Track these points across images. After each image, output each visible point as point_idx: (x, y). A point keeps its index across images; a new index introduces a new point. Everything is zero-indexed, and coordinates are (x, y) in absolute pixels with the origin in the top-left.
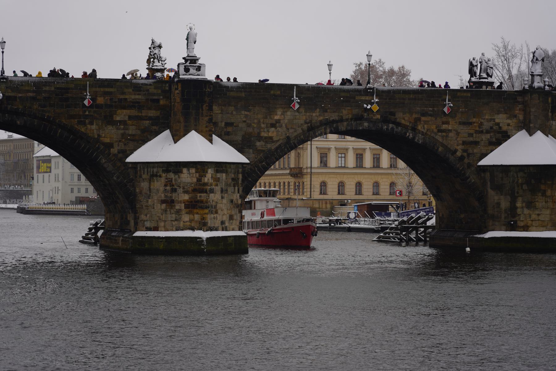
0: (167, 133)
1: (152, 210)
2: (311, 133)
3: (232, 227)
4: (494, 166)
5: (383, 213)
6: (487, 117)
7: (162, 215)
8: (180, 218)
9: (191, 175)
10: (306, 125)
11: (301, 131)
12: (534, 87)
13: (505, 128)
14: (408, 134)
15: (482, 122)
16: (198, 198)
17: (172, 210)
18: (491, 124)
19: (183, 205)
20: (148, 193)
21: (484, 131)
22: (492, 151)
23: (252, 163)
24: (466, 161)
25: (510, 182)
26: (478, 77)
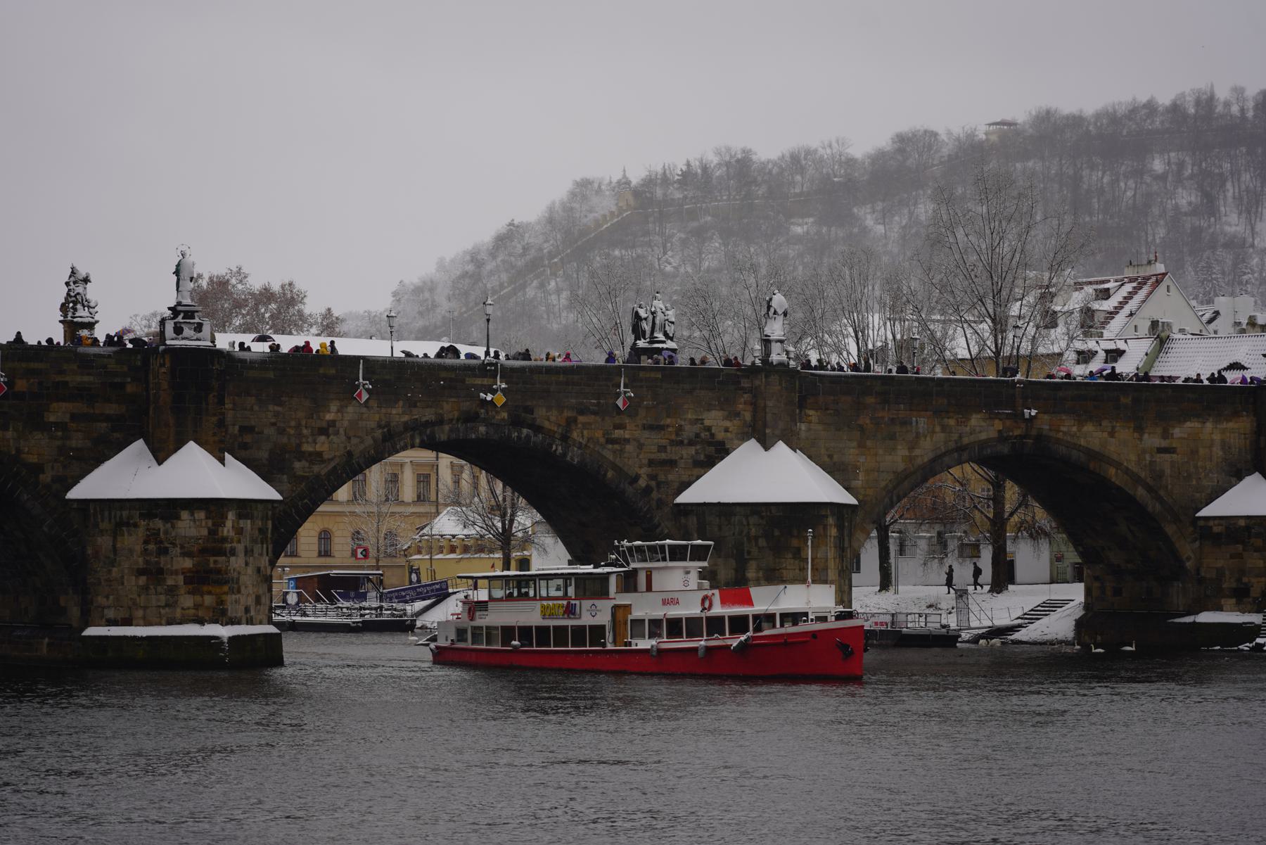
0: (139, 444)
1: (120, 587)
2: (388, 444)
3: (260, 617)
4: (705, 504)
5: (352, 594)
6: (689, 416)
7: (139, 596)
8: (176, 602)
9: (197, 523)
10: (380, 431)
11: (372, 442)
12: (772, 363)
13: (720, 436)
14: (554, 447)
15: (681, 426)
16: (212, 565)
17: (159, 589)
18: (697, 428)
19: (181, 578)
20: (112, 556)
21: (686, 441)
22: (698, 477)
23: (288, 500)
24: (655, 495)
25: (734, 534)
26: (648, 340)
